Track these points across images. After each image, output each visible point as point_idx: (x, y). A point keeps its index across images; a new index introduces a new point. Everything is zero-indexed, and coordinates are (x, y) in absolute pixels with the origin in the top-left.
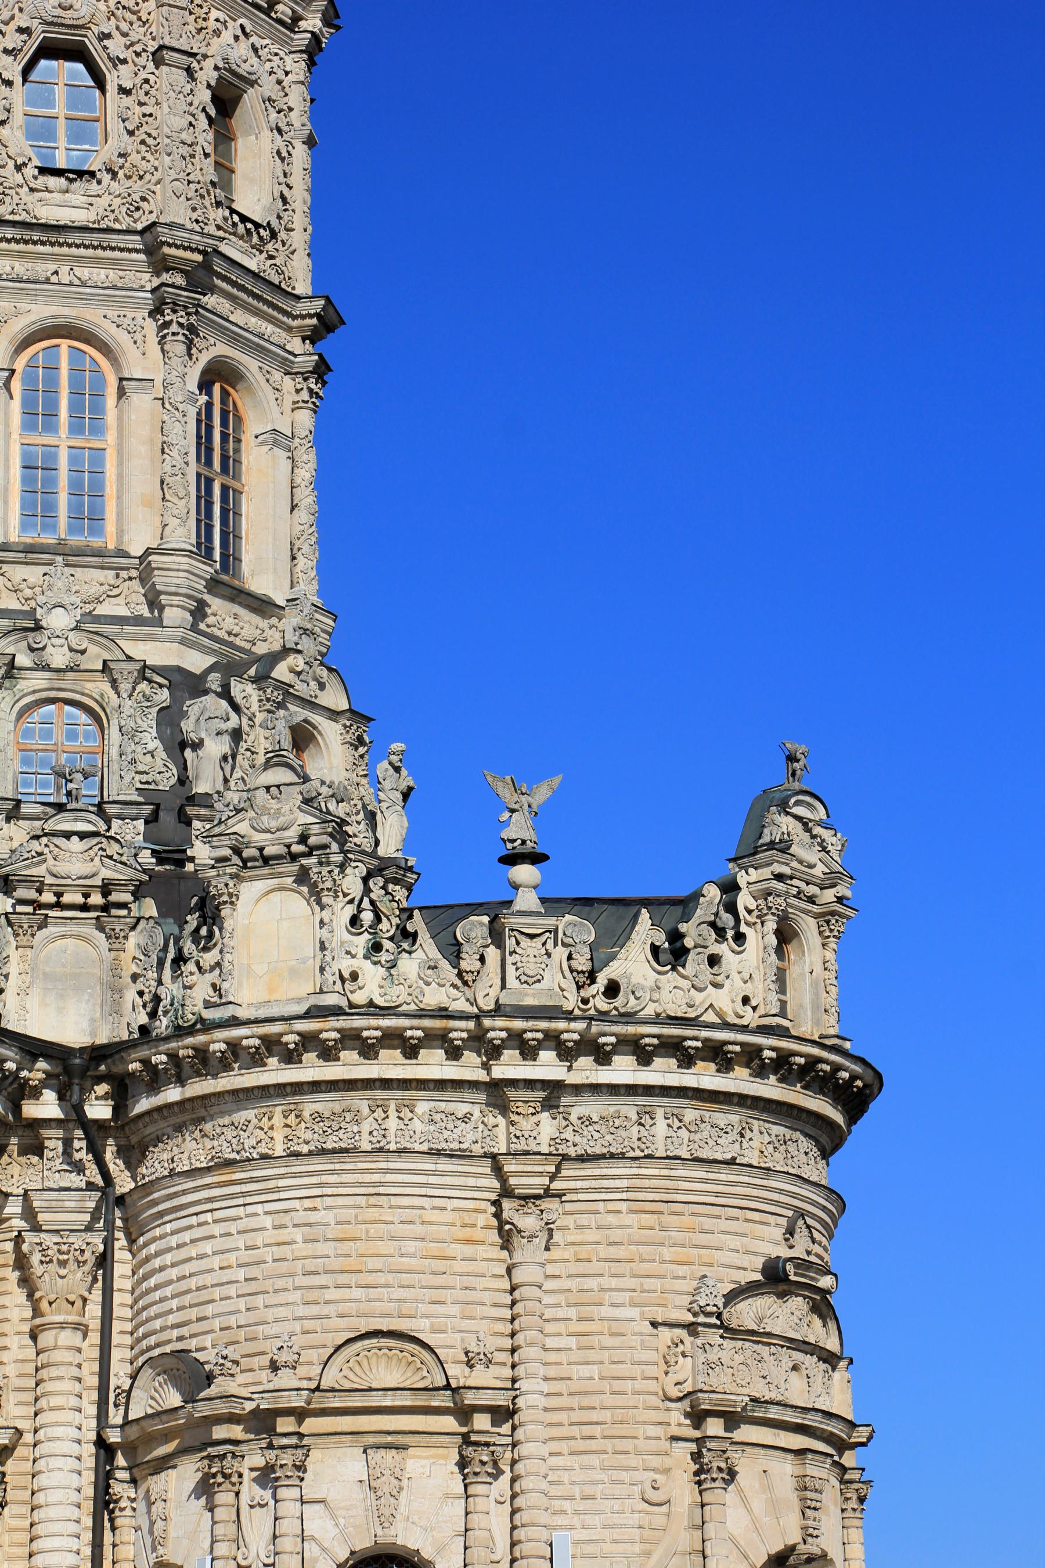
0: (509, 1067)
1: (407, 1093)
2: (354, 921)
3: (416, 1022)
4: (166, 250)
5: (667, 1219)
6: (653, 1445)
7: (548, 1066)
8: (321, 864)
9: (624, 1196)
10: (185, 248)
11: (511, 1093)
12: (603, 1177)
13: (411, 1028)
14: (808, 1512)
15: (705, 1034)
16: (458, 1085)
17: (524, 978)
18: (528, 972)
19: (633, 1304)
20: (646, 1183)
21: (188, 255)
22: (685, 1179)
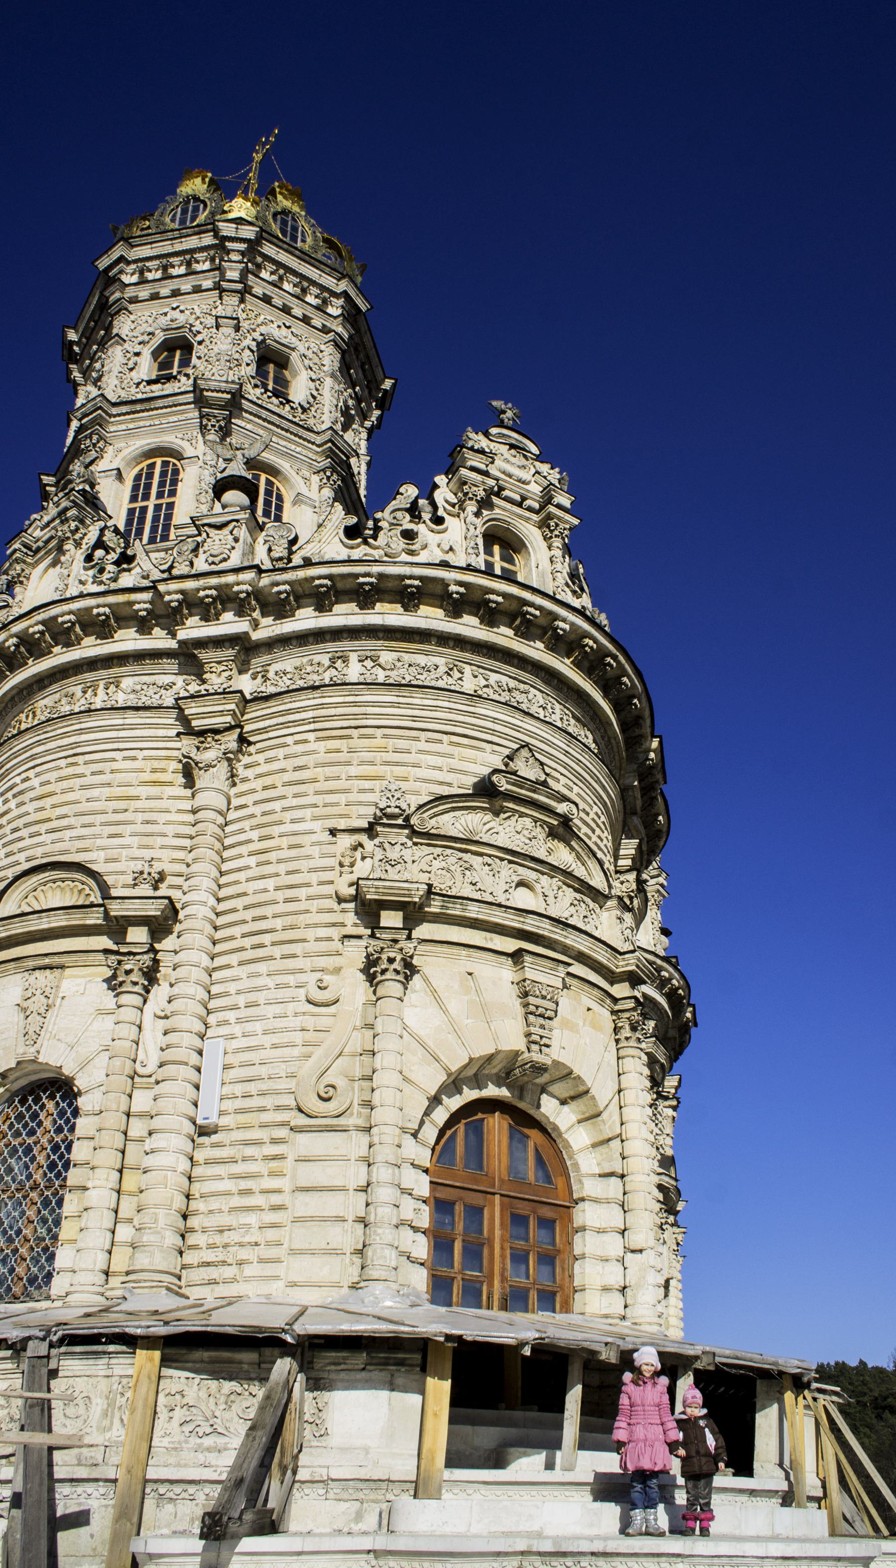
0: (194, 628)
1: (111, 671)
2: (89, 558)
3: (101, 600)
4: (205, 393)
5: (356, 743)
6: (324, 946)
7: (230, 624)
8: (62, 522)
9: (312, 727)
10: (218, 391)
11: (203, 655)
12: (289, 712)
13: (98, 606)
14: (531, 1018)
15: (376, 569)
16: (156, 655)
17: (211, 559)
18: (215, 553)
19: (315, 818)
20: (332, 711)
21: (220, 395)
22: (374, 704)
